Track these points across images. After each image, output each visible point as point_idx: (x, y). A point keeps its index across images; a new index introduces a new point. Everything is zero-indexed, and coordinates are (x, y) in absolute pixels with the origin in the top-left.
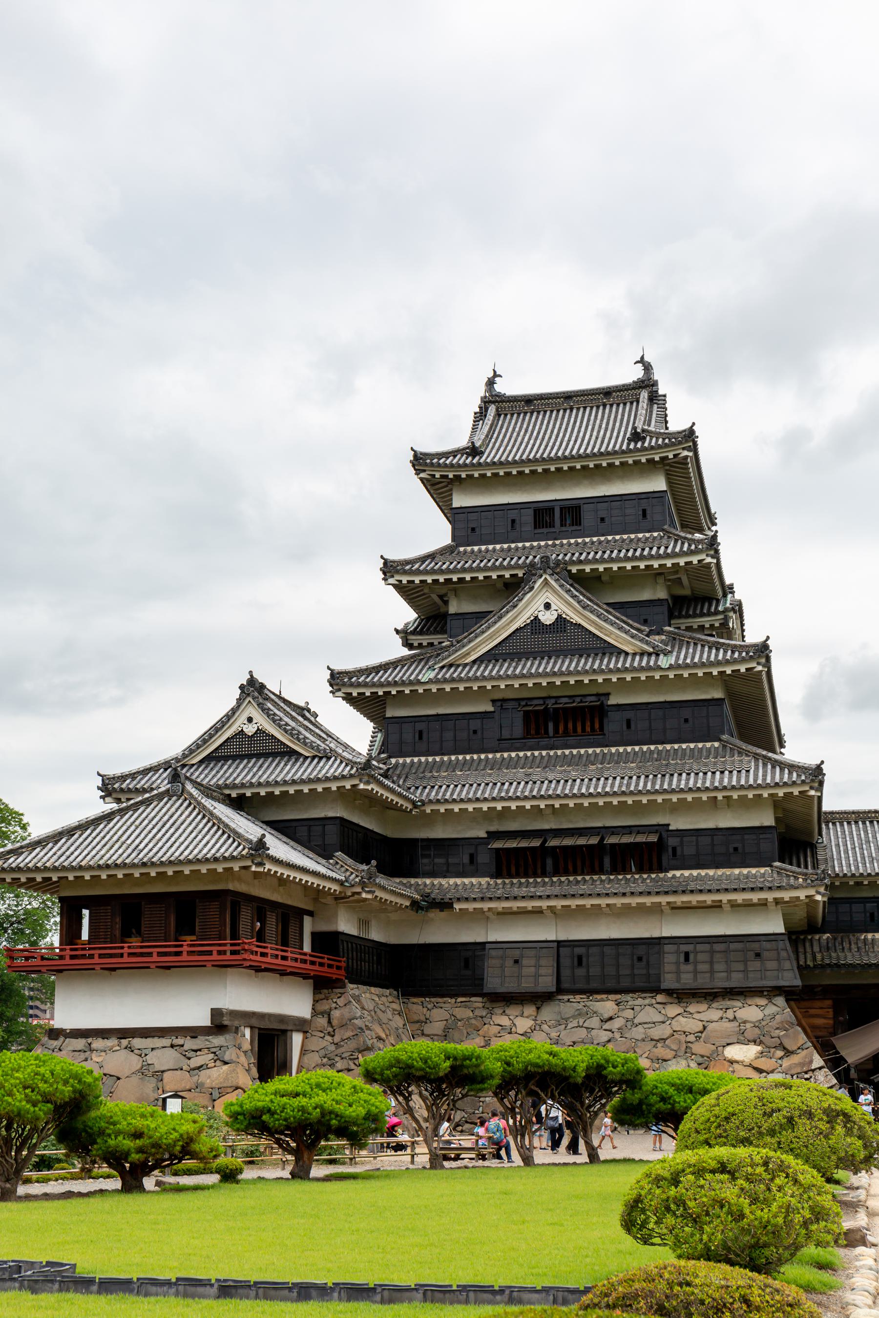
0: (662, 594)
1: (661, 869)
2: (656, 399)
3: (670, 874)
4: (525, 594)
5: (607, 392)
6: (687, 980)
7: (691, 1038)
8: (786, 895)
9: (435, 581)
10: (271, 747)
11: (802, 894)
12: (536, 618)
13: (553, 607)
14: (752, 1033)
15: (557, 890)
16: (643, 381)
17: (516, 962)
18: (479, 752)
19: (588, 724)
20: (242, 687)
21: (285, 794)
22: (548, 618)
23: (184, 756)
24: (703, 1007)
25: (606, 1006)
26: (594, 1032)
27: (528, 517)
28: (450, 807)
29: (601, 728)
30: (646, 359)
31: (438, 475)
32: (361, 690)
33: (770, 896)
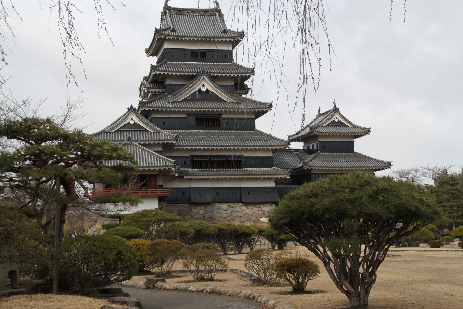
0: (233, 84)
1: (240, 168)
2: (221, 16)
3: (244, 169)
4: (197, 81)
5: (205, 11)
6: (249, 200)
7: (250, 216)
8: (279, 177)
9: (168, 74)
10: (139, 128)
11: (283, 176)
12: (200, 89)
13: (205, 86)
14: (267, 215)
15: (213, 173)
16: (217, 9)
17: (200, 194)
18: (182, 130)
19: (215, 123)
20: (128, 108)
21: (154, 144)
22: (204, 89)
23: (111, 129)
24: (252, 207)
25: (225, 206)
26: (223, 214)
27: (189, 54)
28: (183, 147)
29: (219, 124)
30: (217, 1)
31: (163, 37)
32: (149, 109)
33: (275, 177)
